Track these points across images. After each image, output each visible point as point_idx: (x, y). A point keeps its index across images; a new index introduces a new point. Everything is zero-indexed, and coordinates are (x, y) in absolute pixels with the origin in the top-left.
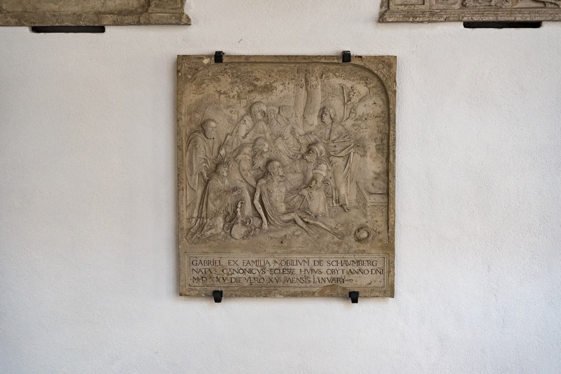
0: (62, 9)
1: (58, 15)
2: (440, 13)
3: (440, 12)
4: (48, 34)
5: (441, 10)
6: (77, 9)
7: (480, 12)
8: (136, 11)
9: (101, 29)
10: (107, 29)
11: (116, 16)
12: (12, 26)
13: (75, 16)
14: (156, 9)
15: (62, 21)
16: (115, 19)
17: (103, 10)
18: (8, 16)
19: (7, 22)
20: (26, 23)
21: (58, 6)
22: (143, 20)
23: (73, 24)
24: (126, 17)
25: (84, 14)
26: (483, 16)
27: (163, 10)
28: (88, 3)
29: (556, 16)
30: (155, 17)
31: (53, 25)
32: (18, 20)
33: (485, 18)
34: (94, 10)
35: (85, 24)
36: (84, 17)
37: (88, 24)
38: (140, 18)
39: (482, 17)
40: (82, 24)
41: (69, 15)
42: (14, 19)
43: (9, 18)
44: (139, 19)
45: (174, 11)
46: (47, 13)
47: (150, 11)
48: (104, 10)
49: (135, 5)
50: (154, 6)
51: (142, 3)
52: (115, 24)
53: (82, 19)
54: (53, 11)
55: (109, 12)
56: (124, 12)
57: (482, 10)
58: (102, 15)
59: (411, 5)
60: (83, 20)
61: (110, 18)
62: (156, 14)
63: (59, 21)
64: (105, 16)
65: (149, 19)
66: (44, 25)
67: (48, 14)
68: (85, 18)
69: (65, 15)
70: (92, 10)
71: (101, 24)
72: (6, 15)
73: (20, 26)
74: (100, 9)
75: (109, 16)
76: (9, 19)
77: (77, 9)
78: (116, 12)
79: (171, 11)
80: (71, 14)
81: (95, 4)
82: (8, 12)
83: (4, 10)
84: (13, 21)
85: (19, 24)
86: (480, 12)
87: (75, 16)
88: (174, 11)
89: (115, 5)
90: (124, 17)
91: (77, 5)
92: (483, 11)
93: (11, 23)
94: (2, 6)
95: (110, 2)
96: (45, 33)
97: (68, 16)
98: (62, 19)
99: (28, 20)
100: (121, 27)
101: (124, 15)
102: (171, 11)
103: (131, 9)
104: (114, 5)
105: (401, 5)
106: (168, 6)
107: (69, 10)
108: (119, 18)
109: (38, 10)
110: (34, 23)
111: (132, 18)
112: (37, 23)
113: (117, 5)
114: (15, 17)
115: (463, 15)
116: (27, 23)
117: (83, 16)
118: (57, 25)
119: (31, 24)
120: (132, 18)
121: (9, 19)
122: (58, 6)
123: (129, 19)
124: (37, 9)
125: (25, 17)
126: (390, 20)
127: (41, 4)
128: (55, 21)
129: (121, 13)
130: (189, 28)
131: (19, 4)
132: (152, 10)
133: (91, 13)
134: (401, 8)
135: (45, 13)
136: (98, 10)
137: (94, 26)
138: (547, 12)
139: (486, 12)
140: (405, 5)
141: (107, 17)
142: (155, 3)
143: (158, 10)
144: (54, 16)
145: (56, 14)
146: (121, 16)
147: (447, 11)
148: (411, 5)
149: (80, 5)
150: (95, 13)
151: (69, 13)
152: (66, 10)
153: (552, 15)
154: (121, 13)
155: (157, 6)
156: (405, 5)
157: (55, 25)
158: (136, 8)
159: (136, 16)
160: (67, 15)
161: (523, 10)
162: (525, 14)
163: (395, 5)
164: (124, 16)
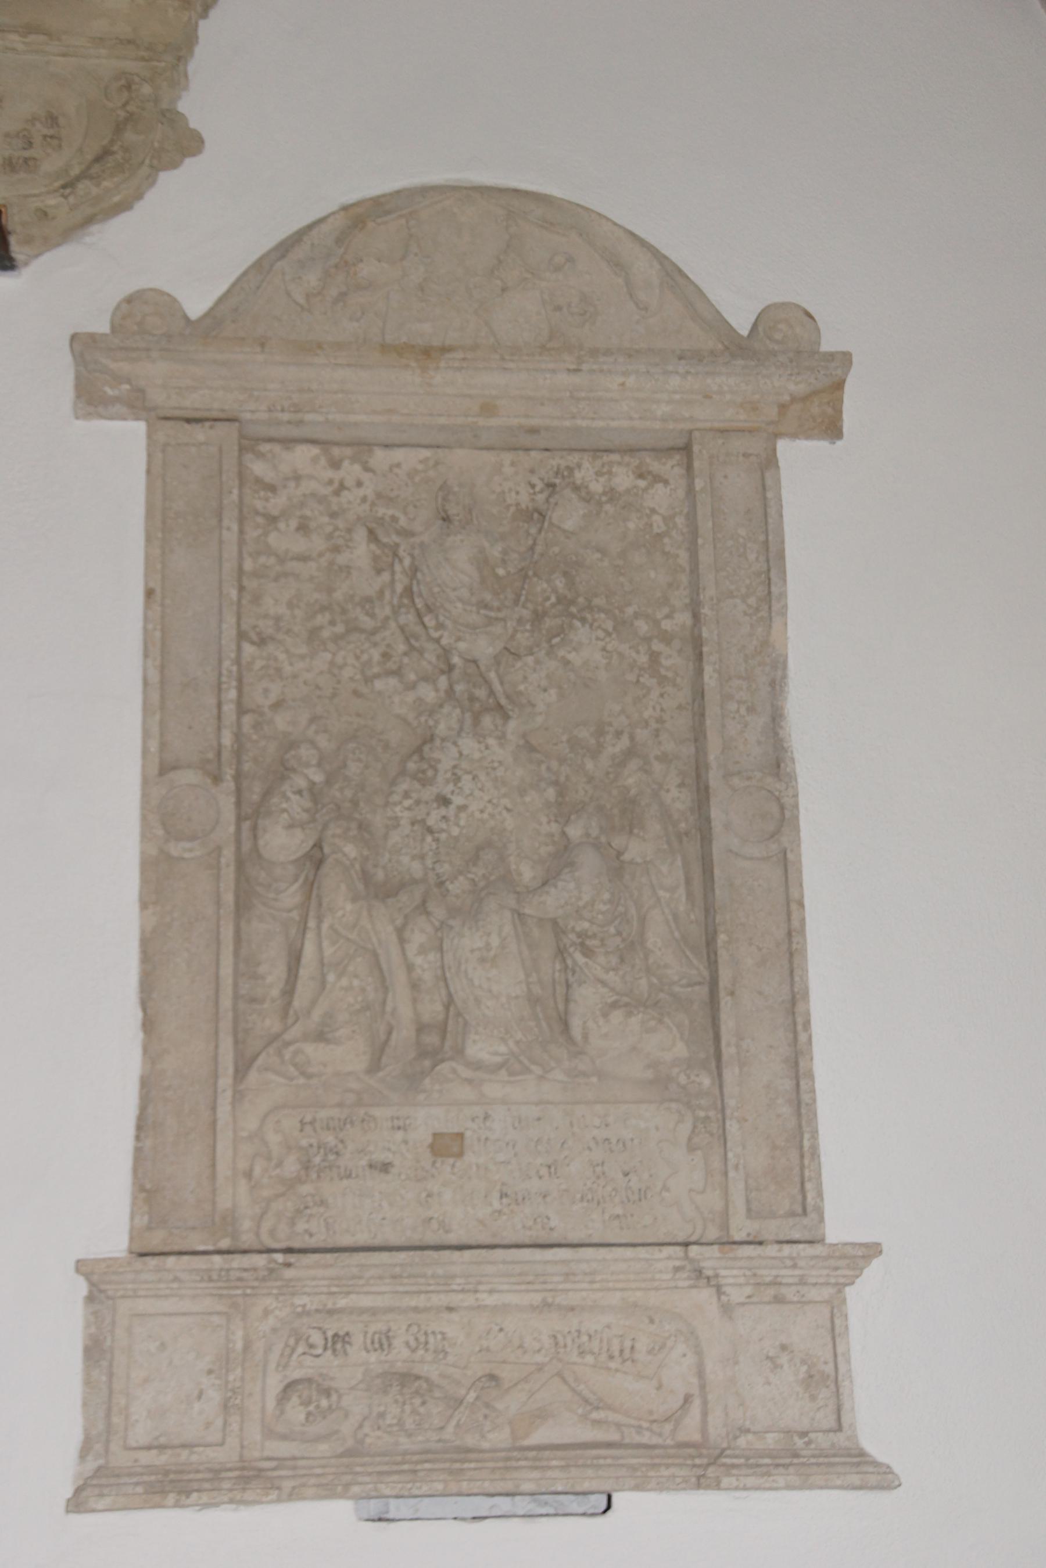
2: (276, 1473)
3: (274, 1469)
5: (281, 1461)
7: (406, 1467)
26: (414, 1481)
29: (652, 1473)
33: (420, 1488)
39: (409, 1486)
57: (415, 1458)
59: (184, 1446)
86: (406, 1467)
92: (417, 1463)
105: (149, 1448)
115: (348, 1478)
126: (100, 1506)
134: (147, 1458)
138: (621, 1461)
139: (427, 1466)
140: (162, 1448)
147: (301, 1463)
148: (184, 1446)
153: (639, 1474)
156: (162, 1448)
161: (547, 1453)
162: (550, 1468)
163: (127, 1448)
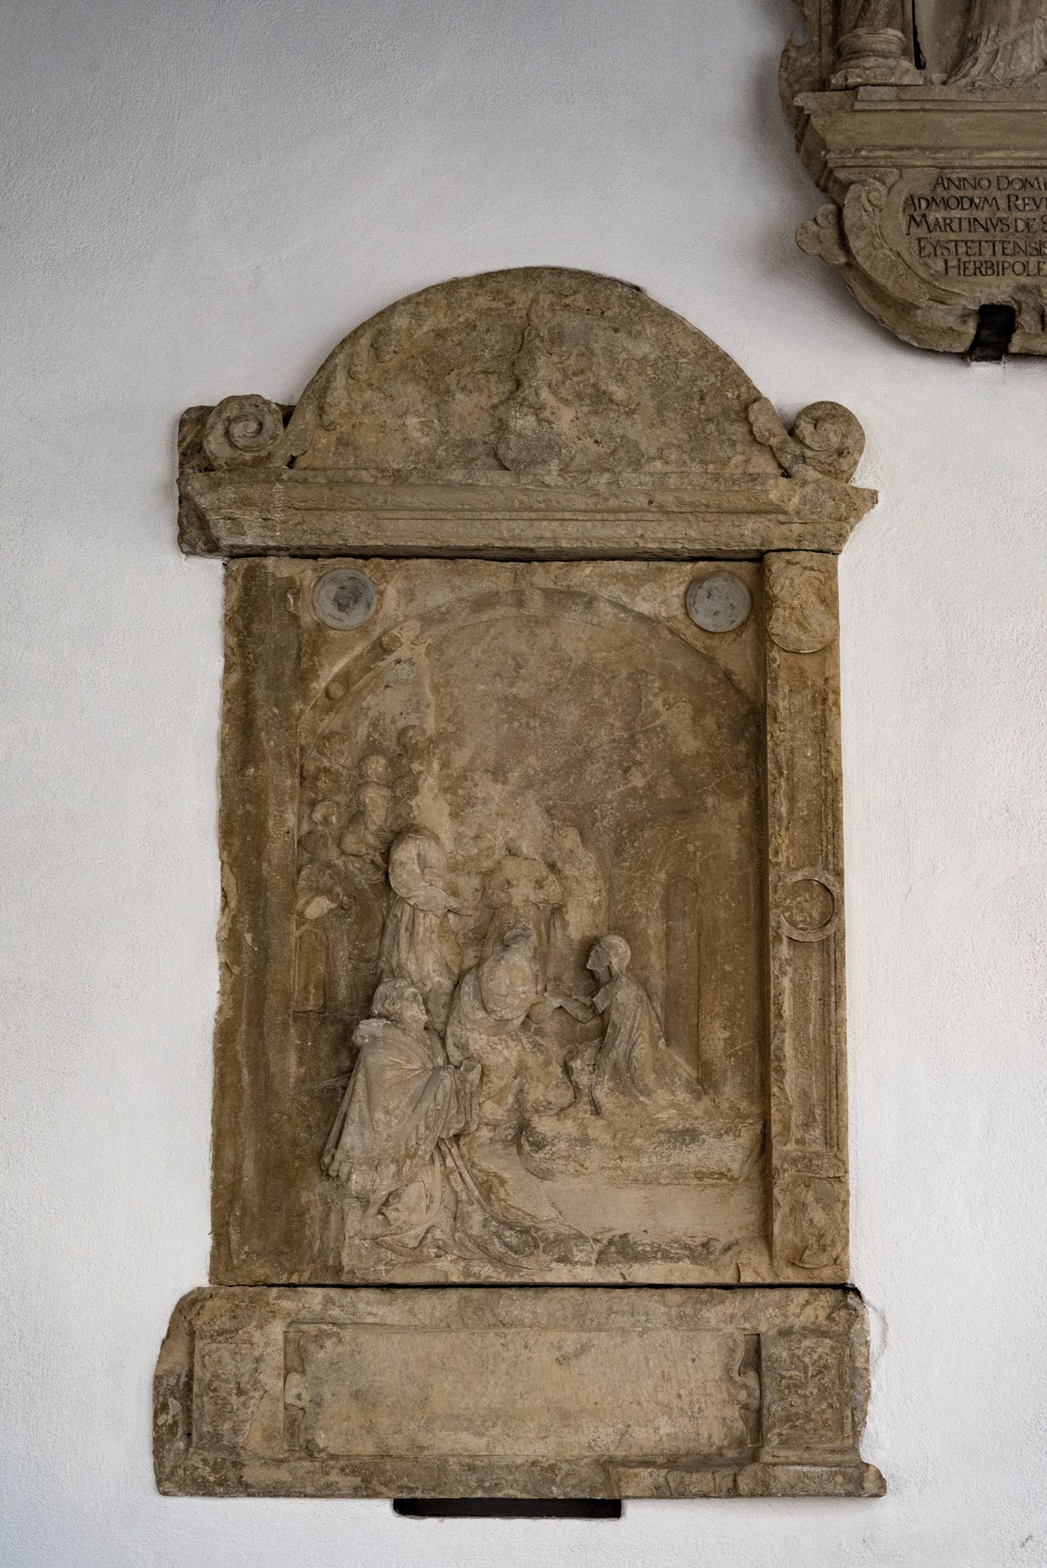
0: (499, 1450)
1: (483, 1467)
4: (450, 1522)
6: (544, 1451)
8: (721, 1455)
9: (611, 1509)
10: (630, 1508)
11: (664, 1472)
12: (343, 1496)
13: (536, 1470)
14: (782, 1453)
15: (496, 1485)
16: (661, 1480)
17: (620, 1453)
18: (333, 1468)
19: (329, 1485)
20: (384, 1490)
21: (485, 1440)
22: (747, 1485)
23: (528, 1493)
24: (695, 1476)
25: (563, 1466)
27: (806, 1455)
28: (577, 1432)
30: (784, 1475)
31: (466, 1496)
32: (362, 1481)
34: (592, 1453)
35: (565, 1494)
36: (563, 1472)
37: (573, 1495)
38: (739, 1479)
40: (556, 1493)
41: (518, 1467)
42: (349, 1478)
43: (334, 1472)
44: (735, 1481)
45: (838, 1458)
46: (451, 1460)
47: (766, 1458)
48: (624, 1453)
49: (715, 1439)
50: (776, 1442)
51: (739, 1433)
52: (660, 1493)
53: (558, 1480)
54: (470, 1456)
55: (640, 1459)
56: (684, 1459)
58: (621, 1469)
60: (562, 1483)
61: (646, 1477)
62: (786, 1467)
63: (487, 1484)
64: (632, 1471)
65: (766, 1485)
66: (441, 1497)
67: (453, 1465)
68: (567, 1475)
69: (507, 1466)
70: (588, 1454)
71: (617, 1496)
72: (327, 1466)
73: (368, 1496)
74: (612, 1449)
75: (644, 1472)
76: (334, 1477)
77: (542, 1450)
78: (661, 1460)
79: (830, 1458)
80: (523, 1465)
81: (596, 1435)
82: (333, 1457)
83: (320, 1451)
84: (346, 1482)
85: (365, 1491)
87: (536, 1470)
88: (838, 1458)
89: (658, 1437)
90: (688, 1475)
91: (543, 1438)
93: (339, 1490)
94: (314, 1439)
95: (643, 1430)
96: (441, 1519)
97: (513, 1469)
98: (497, 1479)
99: (392, 1481)
100: (673, 1502)
101: (689, 1470)
102: (830, 1458)
103: (706, 1450)
104: (654, 1438)
106: (817, 1443)
107: (517, 1453)
108: (674, 1478)
109: (426, 1452)
110: (411, 1489)
111: (714, 1479)
112: (418, 1488)
113: (664, 1439)
114: (353, 1471)
116: (389, 1489)
117: (559, 1469)
118: (479, 1494)
119: (402, 1492)
120: (714, 1479)
121: (334, 1477)
122: (485, 1440)
123: (703, 1480)
124: (421, 1448)
125: (385, 1472)
127: (434, 1435)
128: (473, 1484)
129: (675, 1462)
130: (877, 1503)
131: (368, 1432)
132: (774, 1456)
133: (585, 1461)
135: (446, 1461)
136: (605, 1452)
137: (591, 1501)
141: (636, 1475)
142: (780, 1434)
143: (792, 1455)
144: (472, 1469)
145: (478, 1463)
146: (678, 1473)
149: (552, 1440)
150: (597, 1462)
151: (519, 1461)
152: (508, 1452)
154: (675, 1462)
155: (785, 1443)
157: (474, 1496)
158: (720, 1448)
159: (725, 1471)
160: (509, 1468)
164: (688, 1472)
